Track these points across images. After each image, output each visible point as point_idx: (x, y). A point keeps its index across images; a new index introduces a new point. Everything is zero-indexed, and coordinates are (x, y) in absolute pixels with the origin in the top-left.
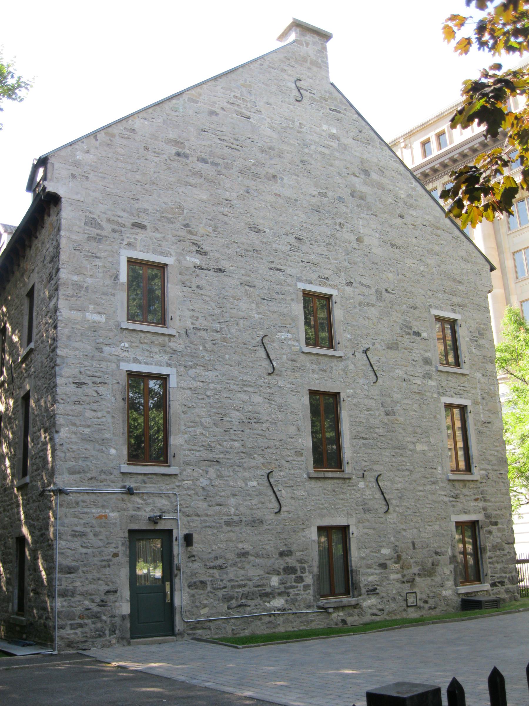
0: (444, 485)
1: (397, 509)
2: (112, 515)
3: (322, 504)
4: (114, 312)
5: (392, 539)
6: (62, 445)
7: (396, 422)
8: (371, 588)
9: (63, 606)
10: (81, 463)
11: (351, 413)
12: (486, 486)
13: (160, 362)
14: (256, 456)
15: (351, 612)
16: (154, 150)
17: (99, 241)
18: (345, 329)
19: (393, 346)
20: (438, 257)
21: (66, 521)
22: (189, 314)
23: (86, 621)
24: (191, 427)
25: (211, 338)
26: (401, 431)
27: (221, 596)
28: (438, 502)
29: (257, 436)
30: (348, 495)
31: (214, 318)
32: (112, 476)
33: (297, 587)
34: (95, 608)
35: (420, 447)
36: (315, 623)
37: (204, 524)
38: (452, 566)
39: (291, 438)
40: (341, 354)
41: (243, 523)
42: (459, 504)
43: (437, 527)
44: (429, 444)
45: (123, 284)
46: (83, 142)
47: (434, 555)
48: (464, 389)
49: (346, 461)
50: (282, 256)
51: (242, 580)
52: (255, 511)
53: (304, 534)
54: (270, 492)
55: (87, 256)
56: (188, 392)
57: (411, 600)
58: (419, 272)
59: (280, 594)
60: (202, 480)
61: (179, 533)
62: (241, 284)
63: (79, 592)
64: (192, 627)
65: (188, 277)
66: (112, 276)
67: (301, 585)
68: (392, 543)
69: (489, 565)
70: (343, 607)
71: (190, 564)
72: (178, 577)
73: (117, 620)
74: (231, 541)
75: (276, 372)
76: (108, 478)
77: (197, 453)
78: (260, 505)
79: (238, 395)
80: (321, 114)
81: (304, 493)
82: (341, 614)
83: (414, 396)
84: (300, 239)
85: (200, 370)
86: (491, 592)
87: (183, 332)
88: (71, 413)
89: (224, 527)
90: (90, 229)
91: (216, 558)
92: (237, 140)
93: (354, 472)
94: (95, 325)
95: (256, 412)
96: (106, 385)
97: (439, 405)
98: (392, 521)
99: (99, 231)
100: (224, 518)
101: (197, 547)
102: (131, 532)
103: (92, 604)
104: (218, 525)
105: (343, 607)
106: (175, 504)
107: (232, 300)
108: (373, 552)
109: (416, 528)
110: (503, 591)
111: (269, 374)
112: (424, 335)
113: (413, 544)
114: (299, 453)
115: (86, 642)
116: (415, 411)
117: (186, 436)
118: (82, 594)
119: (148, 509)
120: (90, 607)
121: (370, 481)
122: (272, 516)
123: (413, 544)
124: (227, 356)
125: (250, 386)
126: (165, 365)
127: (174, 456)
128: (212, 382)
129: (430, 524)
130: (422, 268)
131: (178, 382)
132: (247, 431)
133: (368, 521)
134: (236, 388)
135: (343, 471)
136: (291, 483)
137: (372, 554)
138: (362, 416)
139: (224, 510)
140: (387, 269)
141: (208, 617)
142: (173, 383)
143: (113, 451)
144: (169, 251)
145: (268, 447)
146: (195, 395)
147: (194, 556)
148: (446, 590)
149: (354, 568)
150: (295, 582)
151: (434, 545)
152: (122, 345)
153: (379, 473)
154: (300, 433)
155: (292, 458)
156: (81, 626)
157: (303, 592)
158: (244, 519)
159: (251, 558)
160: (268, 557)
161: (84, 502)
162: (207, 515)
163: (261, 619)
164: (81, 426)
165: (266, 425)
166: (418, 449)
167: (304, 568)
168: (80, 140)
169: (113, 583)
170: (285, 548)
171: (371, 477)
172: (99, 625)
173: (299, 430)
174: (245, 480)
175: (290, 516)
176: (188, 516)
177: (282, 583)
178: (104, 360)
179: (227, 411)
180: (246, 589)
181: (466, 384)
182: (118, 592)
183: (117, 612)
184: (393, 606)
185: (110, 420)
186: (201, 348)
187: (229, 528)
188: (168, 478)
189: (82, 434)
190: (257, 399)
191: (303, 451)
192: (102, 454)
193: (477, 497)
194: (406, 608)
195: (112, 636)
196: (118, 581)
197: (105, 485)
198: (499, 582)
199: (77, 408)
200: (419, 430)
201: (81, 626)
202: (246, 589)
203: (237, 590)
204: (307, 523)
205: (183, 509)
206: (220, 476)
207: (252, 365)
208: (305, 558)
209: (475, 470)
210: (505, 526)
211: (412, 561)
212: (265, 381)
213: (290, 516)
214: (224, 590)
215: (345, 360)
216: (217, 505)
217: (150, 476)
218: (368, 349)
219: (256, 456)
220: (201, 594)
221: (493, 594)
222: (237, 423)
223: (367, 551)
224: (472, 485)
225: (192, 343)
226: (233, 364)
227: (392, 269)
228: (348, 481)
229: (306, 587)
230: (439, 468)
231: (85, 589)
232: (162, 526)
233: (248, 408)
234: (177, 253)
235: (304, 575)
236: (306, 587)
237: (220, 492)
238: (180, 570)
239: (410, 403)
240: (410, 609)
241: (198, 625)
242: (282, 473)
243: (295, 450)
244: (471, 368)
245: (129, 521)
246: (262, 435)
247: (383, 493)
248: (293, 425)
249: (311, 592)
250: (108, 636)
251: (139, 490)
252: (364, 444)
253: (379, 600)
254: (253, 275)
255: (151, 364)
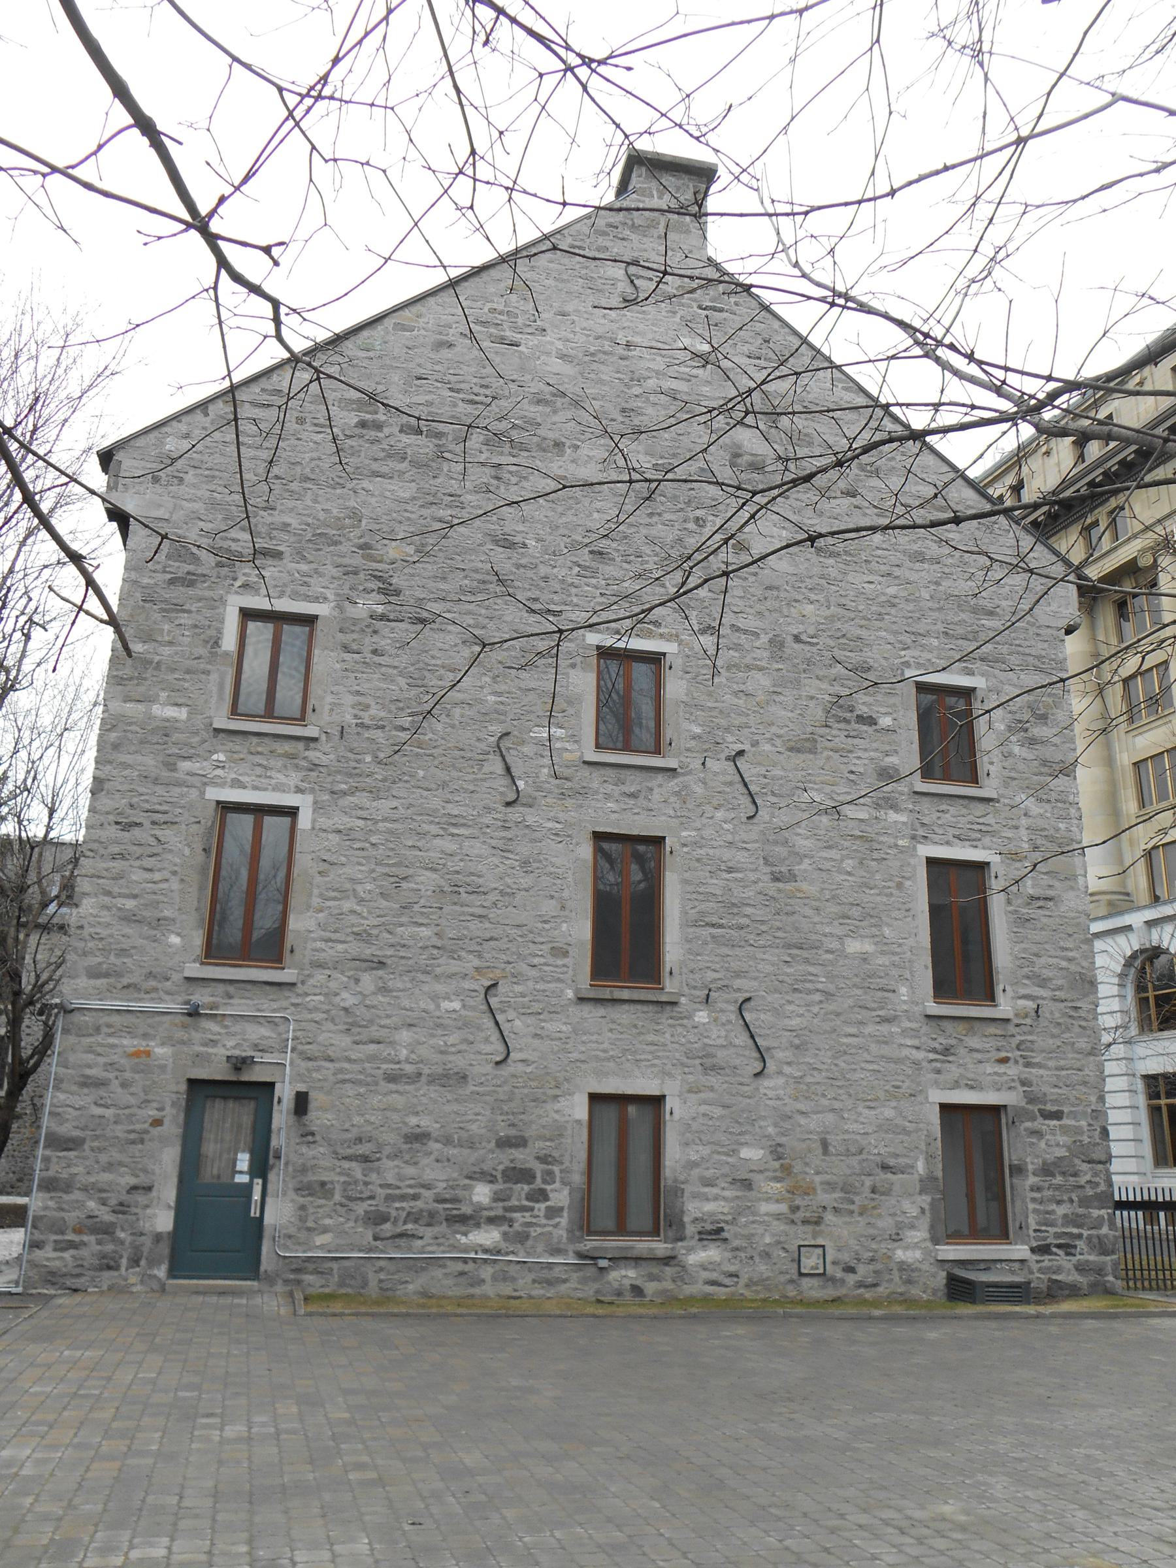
0: (914, 1025)
1: (787, 1070)
2: (159, 1051)
3: (605, 1051)
4: (206, 701)
5: (771, 1130)
6: (81, 927)
7: (799, 895)
8: (709, 1227)
9: (46, 1208)
10: (112, 959)
11: (687, 875)
12: (1031, 1033)
13: (283, 784)
14: (463, 954)
15: (655, 1271)
16: (316, 421)
17: (191, 584)
18: (687, 716)
19: (804, 746)
20: (936, 567)
21: (72, 1058)
22: (349, 699)
23: (85, 1238)
24: (335, 899)
25: (391, 741)
26: (808, 911)
27: (361, 1212)
28: (897, 1061)
29: (469, 918)
30: (667, 1036)
31: (401, 705)
32: (169, 983)
33: (532, 1209)
34: (106, 1216)
35: (854, 946)
36: (568, 1285)
37: (340, 1076)
38: (928, 1198)
39: (545, 922)
40: (672, 763)
41: (424, 1079)
42: (953, 1067)
43: (889, 1113)
44: (881, 941)
45: (226, 654)
46: (180, 421)
47: (879, 1171)
48: (984, 828)
49: (668, 970)
50: (557, 587)
51: (410, 1186)
52: (451, 1058)
53: (557, 1106)
54: (488, 1023)
55: (164, 610)
56: (335, 838)
57: (810, 1262)
58: (883, 598)
59: (491, 1221)
60: (345, 995)
61: (285, 1092)
62: (464, 642)
63: (78, 1185)
64: (293, 1267)
65: (355, 636)
66: (207, 642)
67: (541, 1207)
68: (768, 1137)
69: (1031, 1206)
70: (638, 1260)
71: (304, 1149)
72: (275, 1171)
73: (147, 1242)
74: (396, 1110)
75: (523, 800)
76: (160, 986)
77: (340, 947)
78: (464, 1047)
79: (437, 842)
80: (677, 319)
81: (564, 1028)
82: (631, 1273)
83: (846, 844)
84: (601, 553)
85: (362, 799)
86: (1035, 1267)
87: (335, 731)
88: (105, 874)
89: (382, 1083)
90: (177, 564)
91: (359, 1140)
92: (487, 387)
93: (686, 990)
94: (167, 724)
95: (472, 874)
96: (176, 826)
97: (912, 861)
98: (771, 1094)
99: (191, 568)
100: (384, 1066)
101: (317, 1117)
102: (192, 1082)
103: (103, 1207)
104: (369, 1079)
105: (638, 1260)
106: (284, 1036)
107: (442, 672)
108: (719, 1153)
109: (833, 1110)
110: (1070, 1266)
111: (508, 804)
112: (885, 721)
113: (825, 1145)
114: (560, 952)
115: (78, 1275)
116: (849, 874)
117: (321, 915)
118: (85, 1189)
119: (230, 1043)
120: (96, 1213)
121: (722, 1011)
122: (489, 1068)
123: (825, 1145)
124: (421, 773)
125: (464, 825)
126: (293, 789)
127: (292, 951)
128: (385, 820)
129: (872, 1104)
130: (892, 591)
131: (314, 821)
132: (448, 909)
133: (712, 1089)
134: (434, 829)
135: (662, 989)
136: (537, 1007)
137: (716, 1157)
138: (715, 881)
139: (385, 1051)
140: (800, 597)
141: (329, 1251)
142: (304, 821)
143: (175, 940)
144: (322, 593)
145: (491, 939)
146: (348, 843)
147: (313, 1134)
148: (906, 1248)
149: (670, 1182)
150: (527, 1199)
151: (879, 1147)
152: (215, 757)
153: (747, 995)
154: (567, 913)
155: (542, 960)
156: (72, 1245)
157: (544, 1221)
158: (426, 1071)
159: (435, 1146)
160: (472, 1145)
161: (109, 1026)
162: (349, 1060)
163: (444, 1266)
164: (120, 895)
165: (492, 897)
166: (850, 950)
167: (550, 1173)
168: (176, 417)
169: (145, 1171)
170: (512, 1132)
171: (728, 1002)
172: (110, 1247)
173: (563, 908)
174: (435, 998)
175: (529, 1069)
176: (310, 1059)
177: (497, 1198)
178: (178, 784)
179: (410, 871)
180: (419, 1204)
181: (990, 819)
182: (155, 1189)
183: (146, 1226)
184: (762, 1268)
185: (175, 885)
186: (368, 759)
187: (392, 1086)
188: (275, 988)
189: (120, 909)
190: (477, 848)
191: (569, 948)
192: (155, 945)
193: (1003, 1054)
194: (795, 1277)
195: (131, 1270)
196: (157, 1171)
197: (153, 999)
198: (1059, 1246)
199: (118, 865)
200: (855, 912)
201: (72, 1245)
202: (419, 1204)
203: (397, 1205)
204: (566, 1085)
205: (300, 1047)
206: (384, 990)
207: (472, 788)
208: (556, 1154)
209: (1000, 997)
210: (1083, 1123)
211: (817, 1179)
212: (498, 816)
213: (529, 1069)
214: (369, 1202)
215: (683, 774)
216: (372, 1042)
217: (242, 985)
218: (741, 753)
219: (463, 954)
220: (319, 1207)
221: (1040, 1270)
222: (429, 893)
223: (705, 1151)
224: (992, 1029)
225: (351, 751)
226: (434, 786)
227: (813, 597)
228: (668, 1008)
229: (553, 1212)
230: (903, 990)
231: (92, 1180)
232: (256, 1075)
233: (453, 865)
234: (338, 595)
235: (548, 1187)
236: (553, 1212)
237: (380, 1017)
238: (279, 1158)
239: (838, 857)
240: (806, 1283)
241: (311, 1266)
242: (518, 988)
243: (550, 945)
244: (1006, 785)
245: (190, 1063)
246: (480, 916)
247: (752, 1037)
248: (552, 897)
249: (564, 1221)
250: (123, 1269)
251: (217, 1008)
252: (713, 937)
253: (728, 1255)
254: (491, 625)
255: (266, 789)
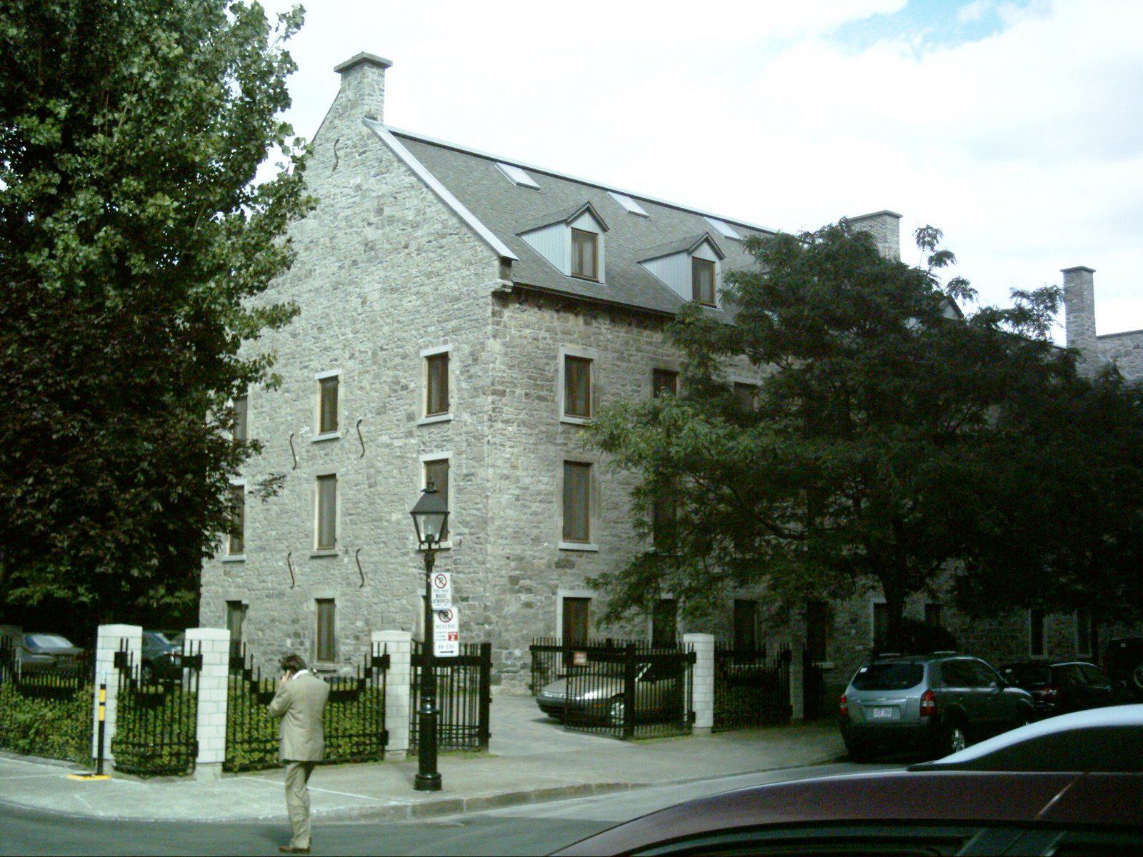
112: (412, 386)
160: (285, 623)
